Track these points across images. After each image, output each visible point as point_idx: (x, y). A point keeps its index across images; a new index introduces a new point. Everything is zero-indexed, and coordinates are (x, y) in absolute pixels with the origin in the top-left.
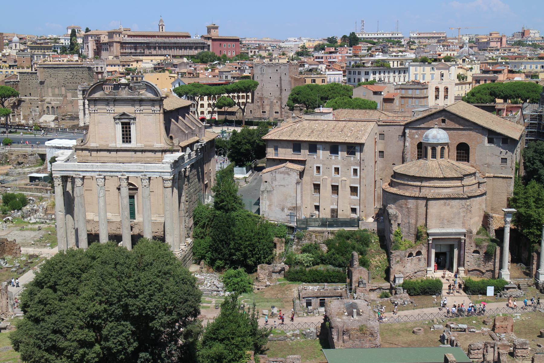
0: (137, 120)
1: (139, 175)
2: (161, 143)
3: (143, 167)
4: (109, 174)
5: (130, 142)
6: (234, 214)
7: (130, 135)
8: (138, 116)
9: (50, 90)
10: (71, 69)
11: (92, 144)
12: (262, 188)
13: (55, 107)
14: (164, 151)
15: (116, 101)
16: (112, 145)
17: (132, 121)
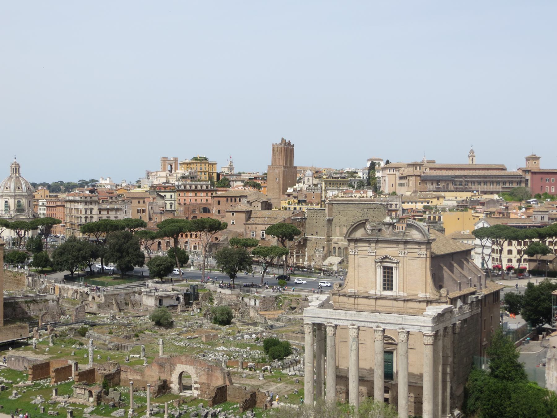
0: (400, 265)
1: (397, 327)
2: (430, 293)
3: (401, 319)
4: (363, 324)
5: (392, 289)
6: (510, 385)
7: (392, 281)
8: (401, 260)
9: (338, 228)
10: (361, 206)
11: (351, 290)
12: (549, 355)
13: (342, 248)
14: (429, 302)
16: (371, 292)
17: (395, 265)
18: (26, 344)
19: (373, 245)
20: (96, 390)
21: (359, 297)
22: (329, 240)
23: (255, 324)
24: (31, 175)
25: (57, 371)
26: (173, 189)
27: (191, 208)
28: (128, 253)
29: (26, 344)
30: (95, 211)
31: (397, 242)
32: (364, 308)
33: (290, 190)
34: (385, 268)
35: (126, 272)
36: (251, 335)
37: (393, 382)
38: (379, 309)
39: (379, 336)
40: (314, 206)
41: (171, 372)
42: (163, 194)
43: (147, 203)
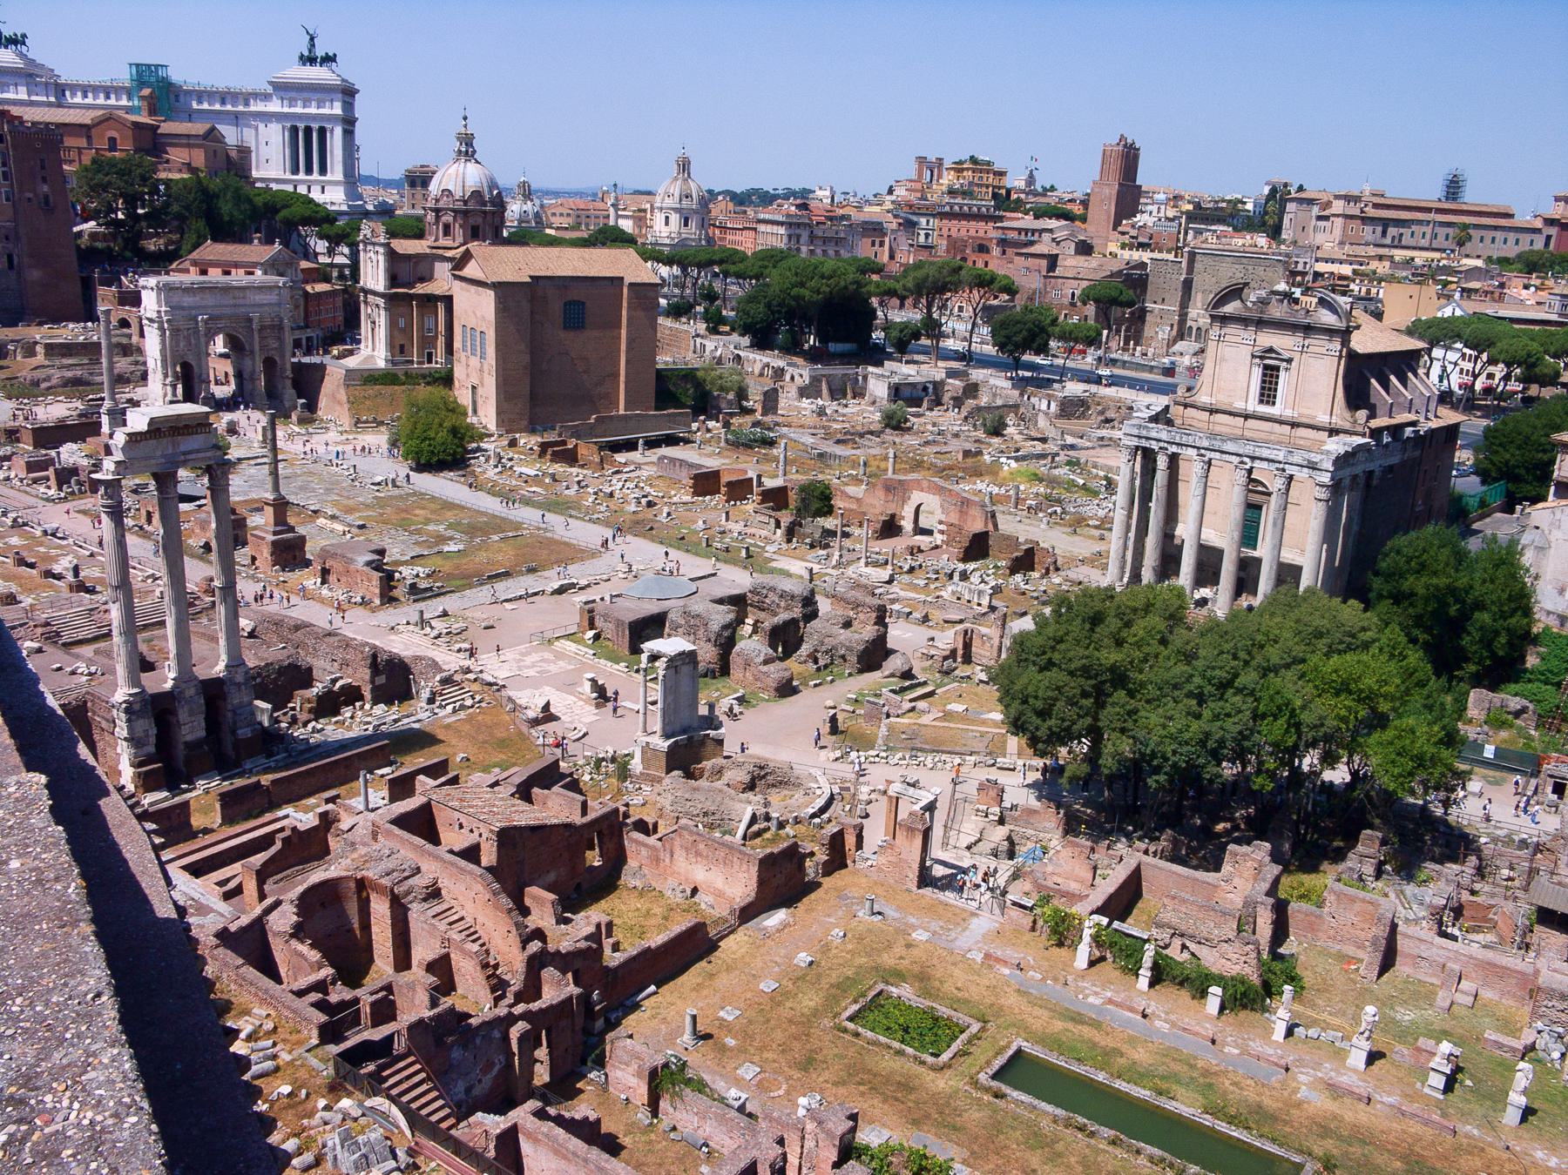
2: (1341, 417)
4: (1217, 455)
8: (1296, 356)
11: (1203, 398)
14: (1333, 432)
15: (1261, 324)
16: (1239, 405)
20: (786, 518)
21: (1217, 411)
22: (1183, 316)
23: (1044, 440)
24: (706, 178)
25: (730, 484)
34: (1266, 367)
38: (1248, 434)
40: (1165, 256)
41: (904, 501)
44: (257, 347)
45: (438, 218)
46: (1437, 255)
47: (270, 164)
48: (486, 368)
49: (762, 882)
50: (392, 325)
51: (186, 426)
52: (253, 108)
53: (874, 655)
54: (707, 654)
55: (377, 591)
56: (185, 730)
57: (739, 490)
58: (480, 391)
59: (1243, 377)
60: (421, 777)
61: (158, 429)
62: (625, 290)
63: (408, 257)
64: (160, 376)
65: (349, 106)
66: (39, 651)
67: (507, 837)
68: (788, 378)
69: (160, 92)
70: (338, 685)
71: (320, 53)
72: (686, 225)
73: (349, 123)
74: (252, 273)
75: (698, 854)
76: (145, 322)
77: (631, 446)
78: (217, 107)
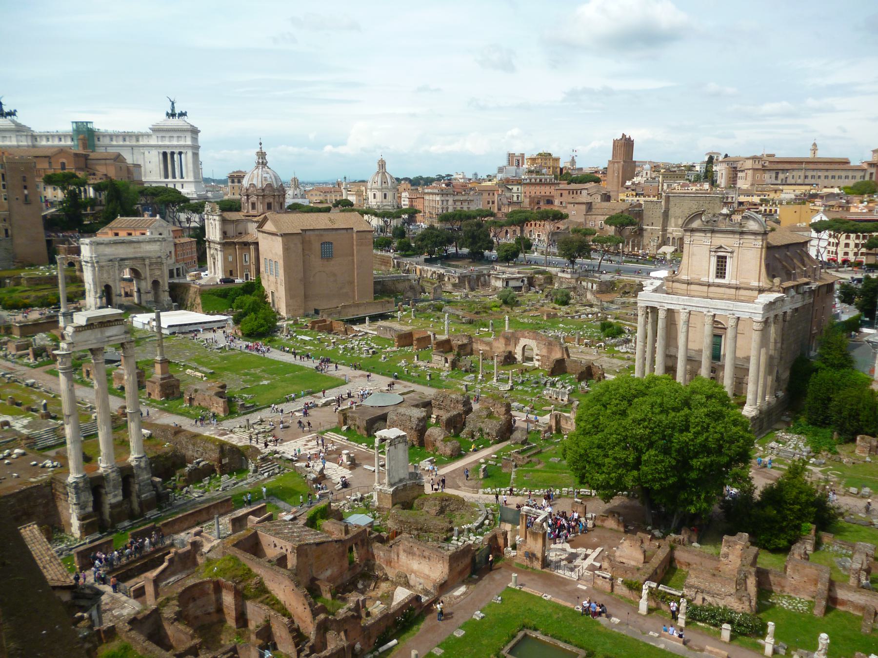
0: (735, 254)
2: (764, 283)
4: (694, 309)
8: (736, 250)
11: (684, 277)
14: (761, 291)
16: (704, 279)
17: (729, 255)
18: (393, 317)
19: (709, 235)
20: (450, 358)
22: (664, 230)
23: (591, 306)
25: (418, 340)
26: (519, 183)
27: (536, 200)
28: (480, 239)
29: (393, 317)
30: (451, 202)
31: (733, 232)
32: (696, 294)
33: (628, 183)
34: (719, 257)
35: (477, 257)
36: (587, 315)
37: (720, 363)
39: (708, 321)
40: (651, 199)
42: (510, 187)
43: (496, 196)
44: (148, 276)
45: (248, 199)
46: (808, 187)
47: (152, 174)
48: (279, 281)
49: (451, 569)
50: (225, 259)
51: (109, 321)
52: (141, 143)
53: (507, 431)
54: (413, 437)
55: (222, 409)
56: (110, 496)
57: (424, 342)
58: (276, 294)
59: (706, 264)
60: (251, 517)
61: (92, 324)
62: (355, 235)
63: (233, 222)
64: (92, 293)
65: (195, 139)
66: (24, 454)
67: (301, 551)
68: (446, 279)
69: (86, 135)
70: (201, 464)
71: (177, 111)
72: (385, 198)
73: (195, 148)
74: (144, 234)
75: (413, 554)
76: (83, 263)
77: (361, 321)
78: (121, 143)
